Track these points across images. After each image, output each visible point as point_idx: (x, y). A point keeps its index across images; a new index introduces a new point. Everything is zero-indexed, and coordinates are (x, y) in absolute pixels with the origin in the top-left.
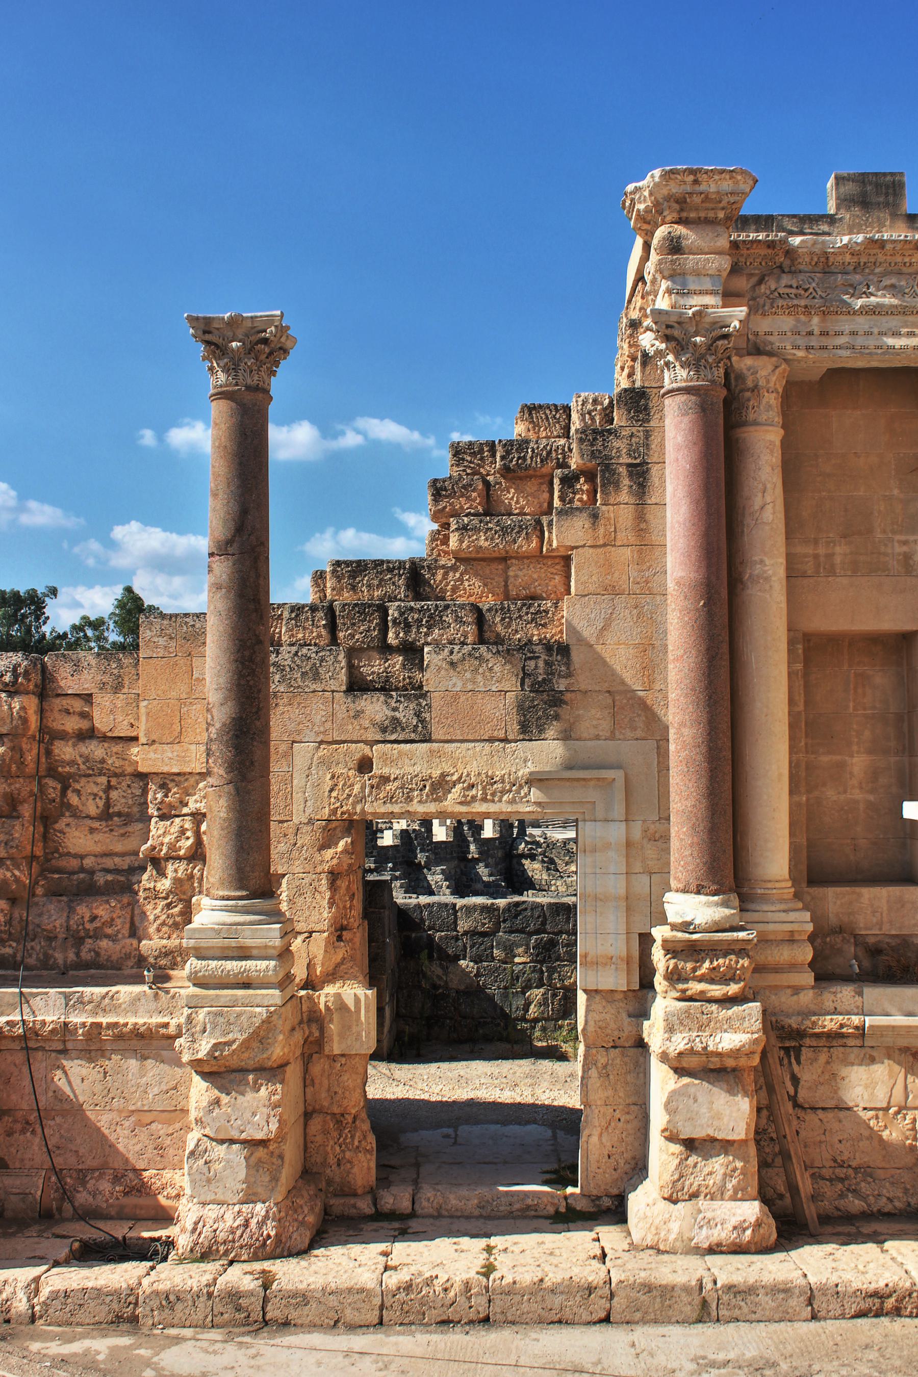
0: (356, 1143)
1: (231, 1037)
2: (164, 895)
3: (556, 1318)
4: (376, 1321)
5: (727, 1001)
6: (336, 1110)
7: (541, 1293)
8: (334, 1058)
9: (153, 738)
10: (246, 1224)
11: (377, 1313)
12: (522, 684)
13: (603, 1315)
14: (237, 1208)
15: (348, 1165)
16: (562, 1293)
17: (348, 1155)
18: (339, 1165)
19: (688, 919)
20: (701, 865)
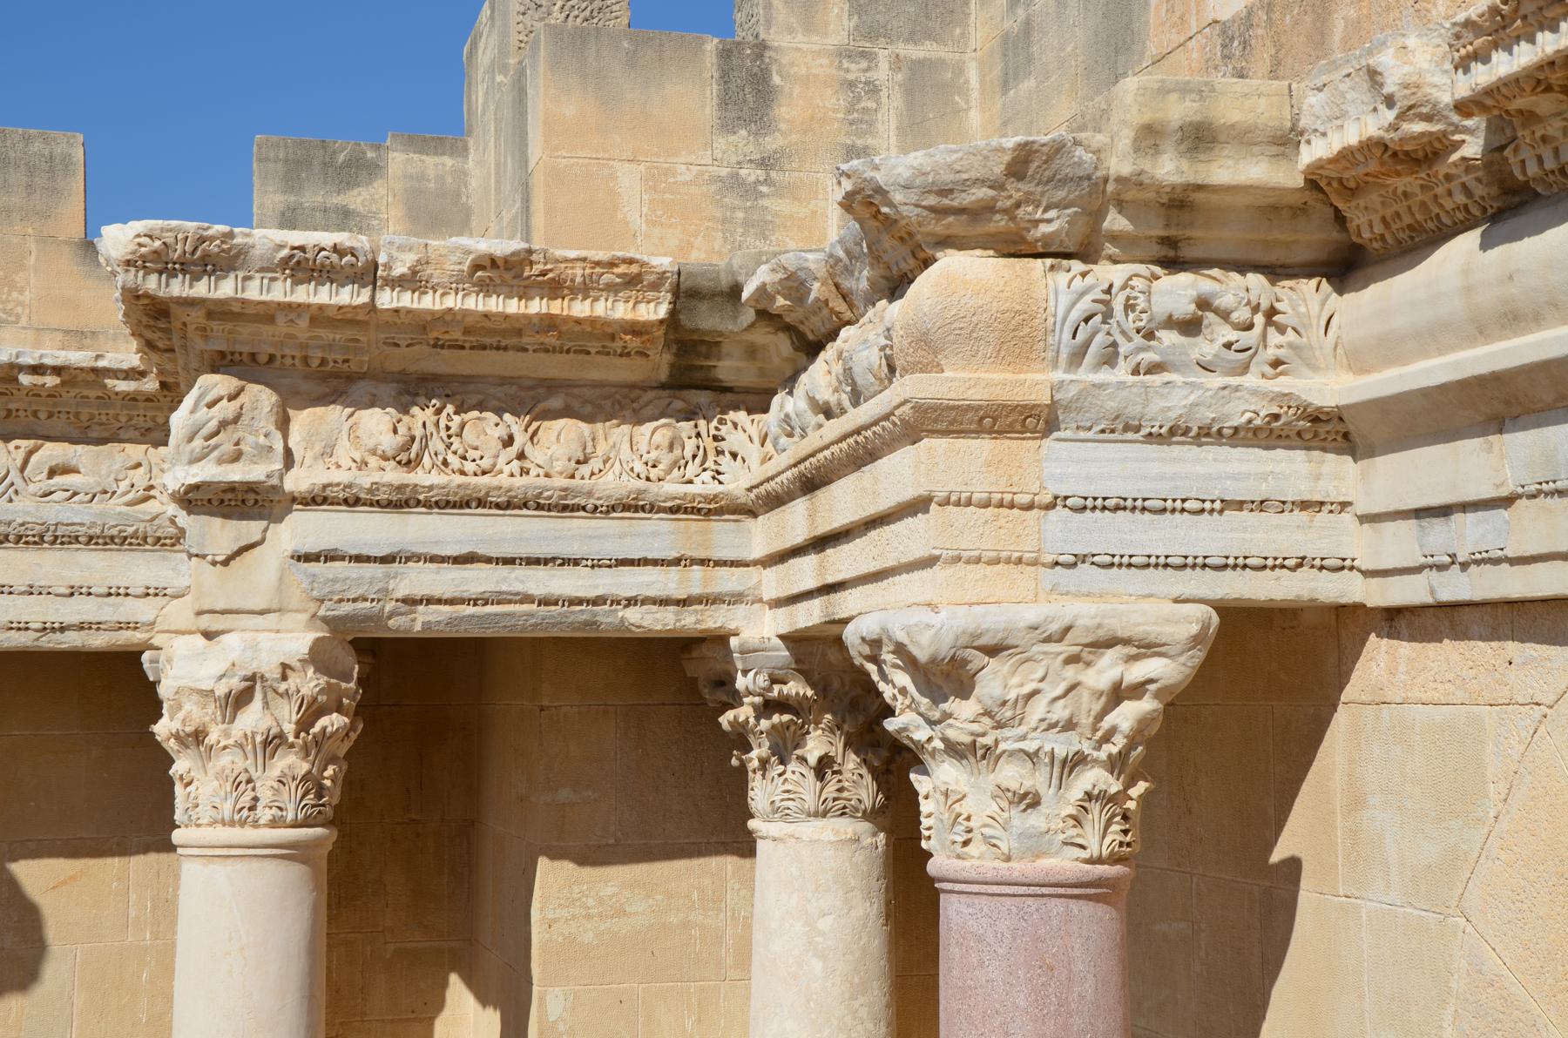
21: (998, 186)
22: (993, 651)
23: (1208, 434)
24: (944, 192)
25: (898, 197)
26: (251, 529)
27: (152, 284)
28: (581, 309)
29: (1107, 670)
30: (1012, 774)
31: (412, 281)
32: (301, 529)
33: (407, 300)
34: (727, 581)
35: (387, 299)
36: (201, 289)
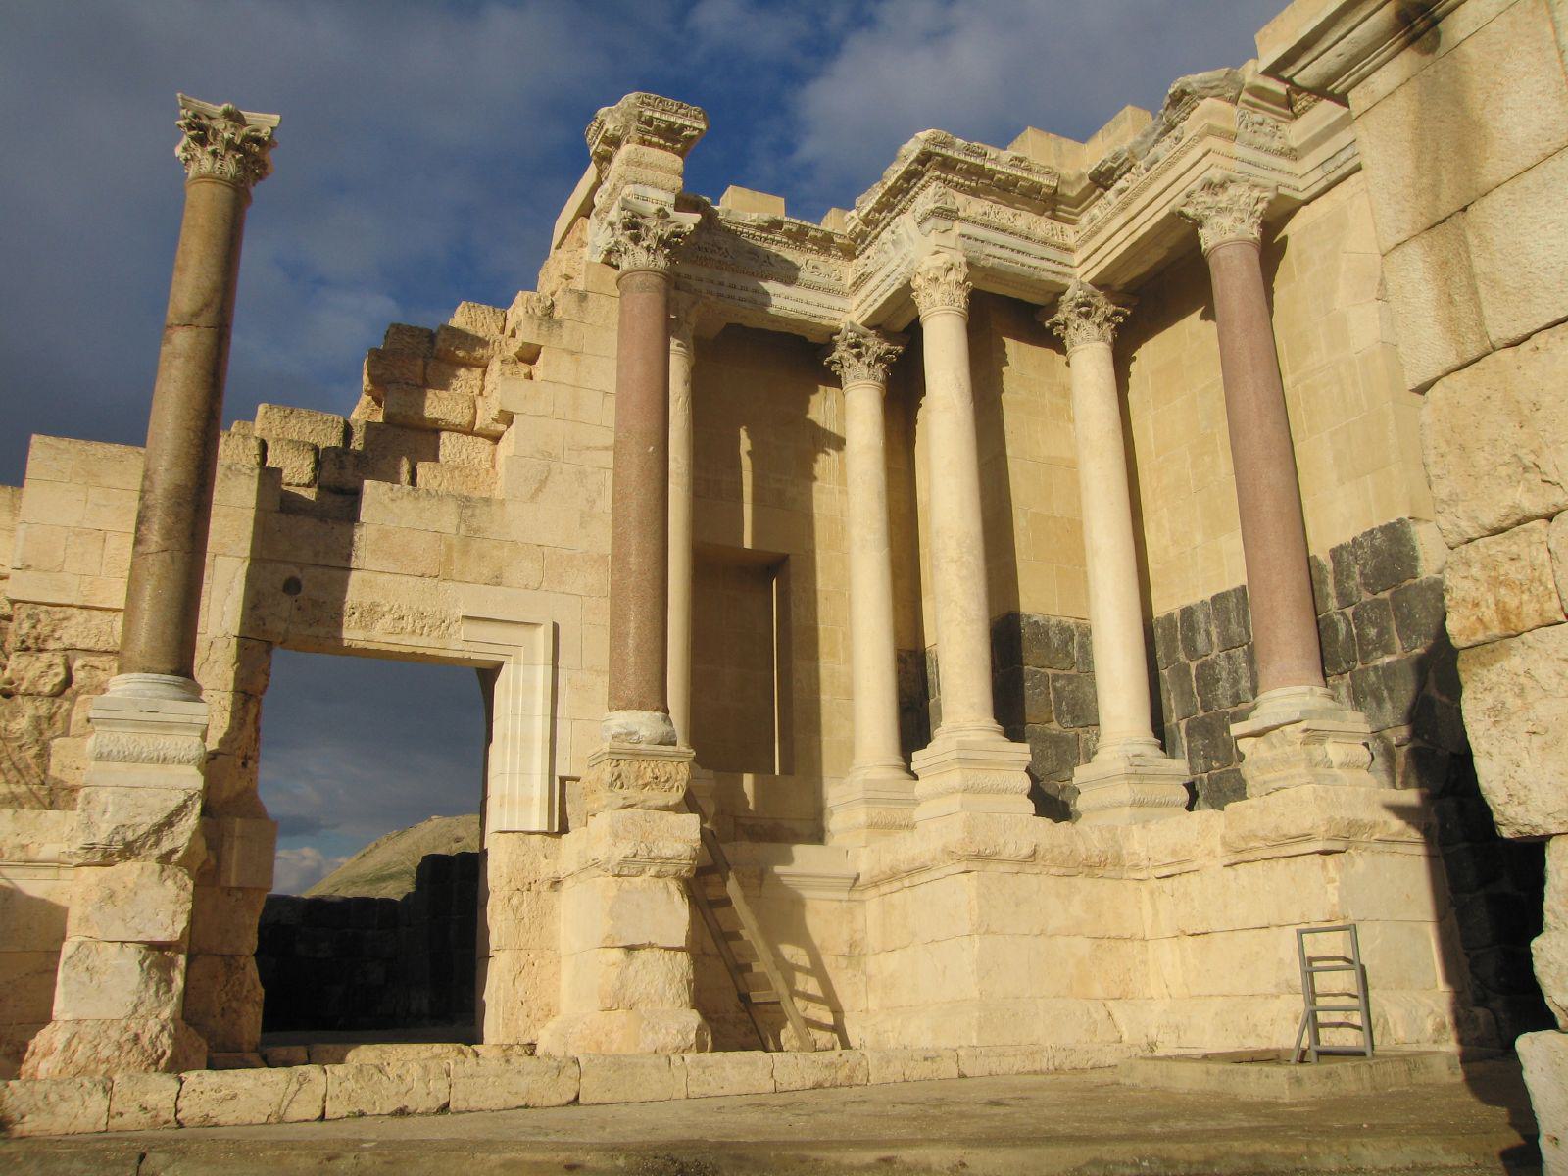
0: (245, 992)
1: (138, 820)
2: (17, 735)
3: (523, 1104)
4: (318, 1114)
5: (667, 808)
6: (227, 950)
7: (508, 1075)
8: (229, 891)
9: (32, 563)
10: (137, 1038)
11: (320, 1103)
12: (458, 528)
13: (572, 1097)
14: (123, 1023)
15: (235, 1016)
16: (528, 1074)
17: (235, 1005)
18: (223, 1016)
19: (633, 730)
20: (644, 683)
21: (1222, 80)
22: (1232, 182)
23: (1268, 151)
24: (1207, 83)
25: (1194, 85)
26: (947, 224)
27: (932, 148)
28: (1035, 178)
29: (1256, 193)
30: (1236, 214)
31: (995, 160)
32: (959, 228)
33: (993, 166)
34: (1067, 270)
35: (988, 165)
36: (943, 151)
